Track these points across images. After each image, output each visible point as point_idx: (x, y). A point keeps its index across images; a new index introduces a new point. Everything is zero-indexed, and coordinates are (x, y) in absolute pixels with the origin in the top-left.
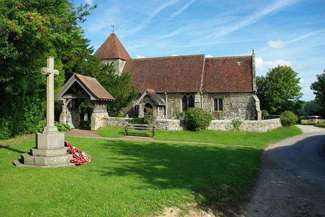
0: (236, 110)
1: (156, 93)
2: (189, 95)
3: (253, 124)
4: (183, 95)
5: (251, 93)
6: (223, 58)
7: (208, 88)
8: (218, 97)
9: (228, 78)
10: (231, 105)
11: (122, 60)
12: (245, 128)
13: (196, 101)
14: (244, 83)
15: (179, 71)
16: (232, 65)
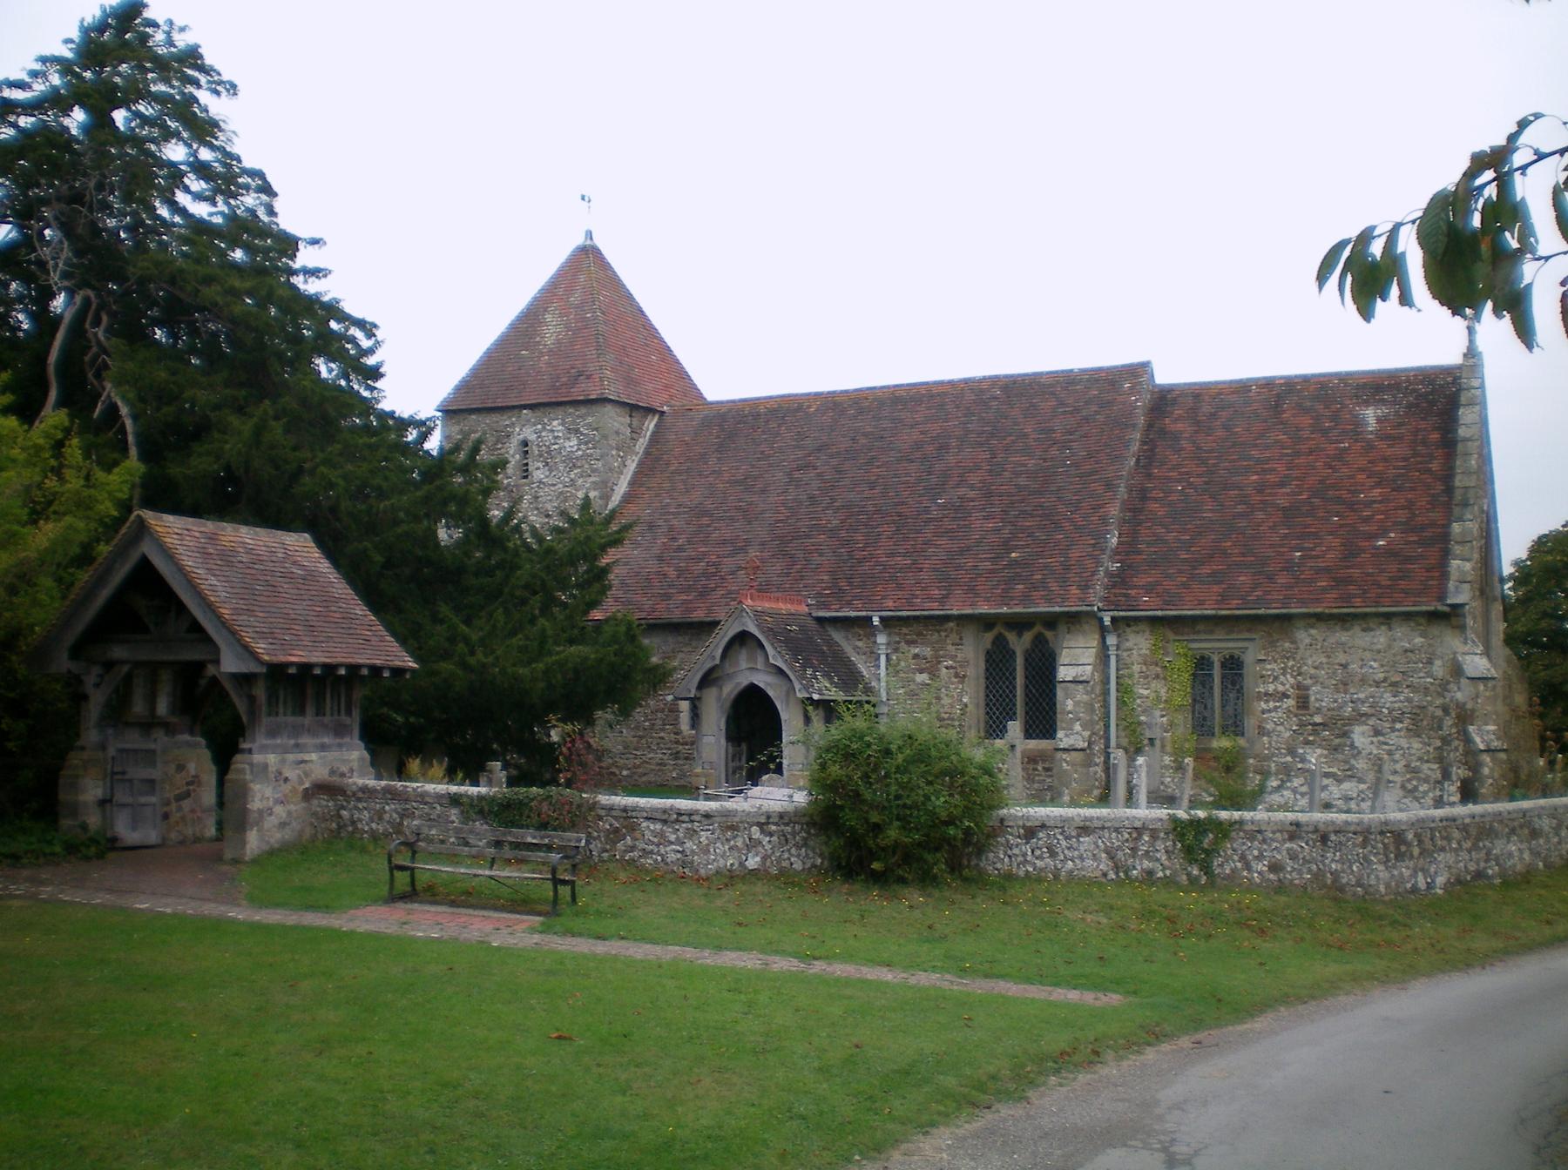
0: (1334, 731)
1: (820, 620)
2: (1028, 636)
3: (1324, 839)
4: (989, 637)
5: (1434, 617)
7: (1149, 590)
8: (1216, 646)
9: (1289, 513)
10: (1303, 703)
11: (633, 408)
12: (1261, 866)
13: (1064, 673)
14: (1390, 552)
15: (974, 479)
16: (1325, 432)
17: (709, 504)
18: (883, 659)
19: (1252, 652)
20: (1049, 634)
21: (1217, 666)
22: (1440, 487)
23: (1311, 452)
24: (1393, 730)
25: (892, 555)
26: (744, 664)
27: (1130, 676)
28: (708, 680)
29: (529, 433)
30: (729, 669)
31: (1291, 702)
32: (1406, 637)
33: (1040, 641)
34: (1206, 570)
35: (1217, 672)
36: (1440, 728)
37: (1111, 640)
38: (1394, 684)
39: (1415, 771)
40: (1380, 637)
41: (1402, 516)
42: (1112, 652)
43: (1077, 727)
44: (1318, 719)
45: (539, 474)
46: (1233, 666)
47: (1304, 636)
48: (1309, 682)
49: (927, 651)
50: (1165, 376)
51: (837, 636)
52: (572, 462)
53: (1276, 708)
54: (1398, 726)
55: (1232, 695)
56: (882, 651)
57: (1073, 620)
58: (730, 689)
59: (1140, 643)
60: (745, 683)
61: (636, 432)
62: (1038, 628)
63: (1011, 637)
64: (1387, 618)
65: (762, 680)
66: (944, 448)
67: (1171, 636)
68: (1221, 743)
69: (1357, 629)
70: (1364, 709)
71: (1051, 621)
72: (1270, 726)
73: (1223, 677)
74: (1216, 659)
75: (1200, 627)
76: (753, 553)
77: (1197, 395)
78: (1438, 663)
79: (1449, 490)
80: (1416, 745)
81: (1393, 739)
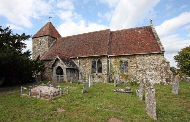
1: (71, 58)
2: (98, 59)
4: (92, 60)
6: (125, 30)
8: (124, 60)
9: (131, 42)
10: (138, 67)
11: (53, 37)
13: (103, 64)
14: (149, 46)
15: (90, 42)
17: (60, 47)
18: (79, 64)
19: (129, 60)
20: (100, 59)
21: (124, 63)
22: (153, 38)
23: (132, 36)
24: (152, 71)
25: (80, 50)
26: (58, 63)
27: (112, 64)
28: (53, 65)
29: (41, 40)
30: (56, 64)
31: (136, 67)
32: (153, 57)
33: (99, 60)
34: (121, 50)
35: (124, 63)
36: (160, 71)
37: (109, 59)
38: (152, 64)
39: (156, 77)
40: (149, 57)
41: (149, 41)
42: (109, 61)
43: (105, 71)
44: (140, 70)
45: (42, 44)
46: (126, 63)
47: (137, 58)
48: (138, 64)
49: (85, 62)
50: (112, 30)
51: (73, 60)
52: (45, 42)
53: (133, 68)
54: (153, 70)
55: (126, 67)
56: (79, 62)
57: (104, 56)
58: (56, 67)
59: (113, 60)
60: (58, 65)
61: (53, 40)
62: (99, 58)
63: (95, 60)
64: (150, 54)
65: (60, 65)
66: (87, 39)
67: (117, 58)
68: (125, 73)
69: (145, 56)
70: (147, 68)
71: (101, 57)
72: (133, 71)
73: (125, 64)
74: (124, 62)
75: (121, 57)
76: (64, 51)
77: (116, 32)
78: (159, 61)
79: (155, 38)
80: (156, 73)
81: (152, 72)
